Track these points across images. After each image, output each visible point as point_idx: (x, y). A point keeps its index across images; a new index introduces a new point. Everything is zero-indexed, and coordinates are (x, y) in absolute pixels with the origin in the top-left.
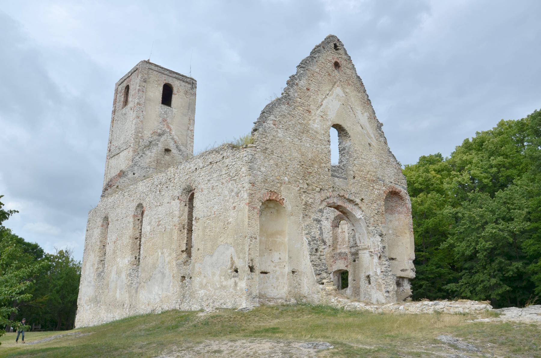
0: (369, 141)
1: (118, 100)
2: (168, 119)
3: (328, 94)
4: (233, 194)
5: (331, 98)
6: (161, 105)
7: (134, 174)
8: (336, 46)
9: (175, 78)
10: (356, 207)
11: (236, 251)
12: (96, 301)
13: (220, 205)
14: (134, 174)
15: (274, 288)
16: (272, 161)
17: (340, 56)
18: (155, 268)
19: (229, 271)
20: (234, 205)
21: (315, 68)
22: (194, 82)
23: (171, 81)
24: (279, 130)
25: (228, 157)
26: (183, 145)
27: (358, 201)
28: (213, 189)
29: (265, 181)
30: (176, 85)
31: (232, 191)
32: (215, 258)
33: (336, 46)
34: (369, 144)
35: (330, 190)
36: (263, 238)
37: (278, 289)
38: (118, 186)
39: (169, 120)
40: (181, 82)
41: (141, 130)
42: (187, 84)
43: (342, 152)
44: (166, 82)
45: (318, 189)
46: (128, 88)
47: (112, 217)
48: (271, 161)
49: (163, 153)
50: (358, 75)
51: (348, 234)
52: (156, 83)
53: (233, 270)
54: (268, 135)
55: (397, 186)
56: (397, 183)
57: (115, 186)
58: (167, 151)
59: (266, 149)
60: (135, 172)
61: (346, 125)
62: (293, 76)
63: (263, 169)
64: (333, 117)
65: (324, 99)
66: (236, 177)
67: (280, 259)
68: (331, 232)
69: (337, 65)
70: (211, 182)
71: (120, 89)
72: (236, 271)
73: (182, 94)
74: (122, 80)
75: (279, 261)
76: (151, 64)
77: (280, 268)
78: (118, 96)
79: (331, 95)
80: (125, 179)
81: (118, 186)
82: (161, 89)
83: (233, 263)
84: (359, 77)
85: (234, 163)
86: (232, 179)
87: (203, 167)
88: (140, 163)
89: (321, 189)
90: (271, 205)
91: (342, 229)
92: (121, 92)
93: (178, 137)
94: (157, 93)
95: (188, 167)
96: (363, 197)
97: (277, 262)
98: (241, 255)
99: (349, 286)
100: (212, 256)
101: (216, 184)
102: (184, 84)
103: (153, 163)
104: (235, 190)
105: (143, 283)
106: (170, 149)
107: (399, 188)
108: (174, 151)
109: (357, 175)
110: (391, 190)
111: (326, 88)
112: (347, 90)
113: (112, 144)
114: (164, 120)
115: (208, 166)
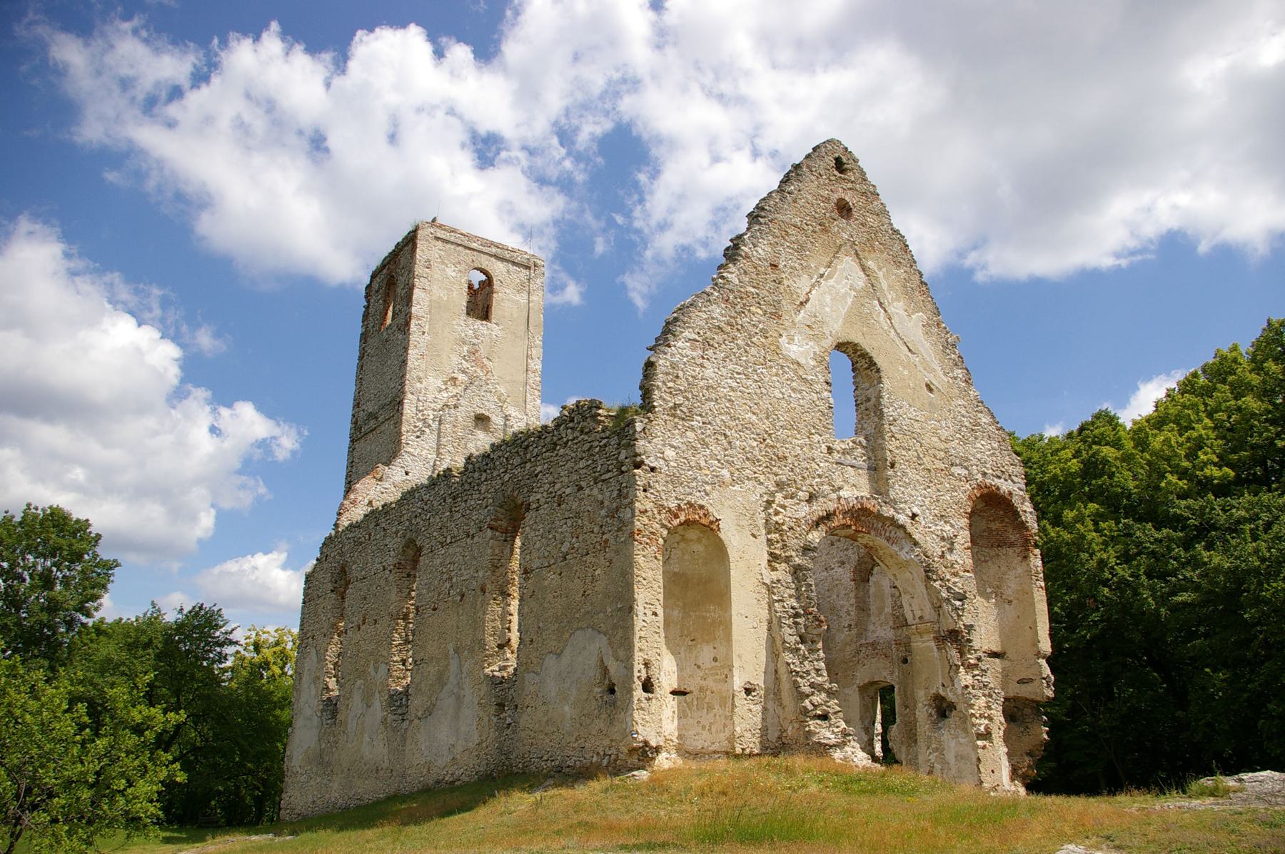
0: (930, 378)
3: (822, 276)
5: (831, 282)
6: (464, 317)
7: (407, 473)
8: (839, 165)
10: (900, 533)
11: (610, 643)
12: (322, 761)
14: (407, 473)
15: (704, 727)
17: (850, 185)
18: (443, 684)
19: (597, 690)
21: (789, 215)
23: (486, 262)
24: (706, 363)
27: (902, 519)
30: (498, 269)
32: (566, 659)
33: (839, 165)
34: (928, 386)
36: (676, 613)
37: (713, 730)
39: (483, 351)
41: (421, 375)
43: (863, 407)
46: (391, 283)
47: (355, 571)
48: (689, 433)
49: (471, 424)
50: (896, 226)
53: (605, 687)
54: (681, 374)
56: (999, 473)
57: (366, 501)
61: (867, 344)
62: (740, 237)
63: (670, 453)
64: (837, 328)
65: (813, 286)
67: (715, 660)
68: (852, 595)
69: (844, 209)
72: (612, 691)
75: (714, 664)
76: (441, 226)
77: (715, 681)
79: (830, 277)
83: (605, 671)
84: (896, 232)
85: (604, 441)
90: (692, 534)
96: (916, 510)
97: (708, 666)
98: (621, 653)
99: (898, 720)
100: (559, 655)
105: (416, 721)
106: (487, 414)
107: (1005, 486)
110: (985, 491)
111: (816, 261)
112: (870, 264)
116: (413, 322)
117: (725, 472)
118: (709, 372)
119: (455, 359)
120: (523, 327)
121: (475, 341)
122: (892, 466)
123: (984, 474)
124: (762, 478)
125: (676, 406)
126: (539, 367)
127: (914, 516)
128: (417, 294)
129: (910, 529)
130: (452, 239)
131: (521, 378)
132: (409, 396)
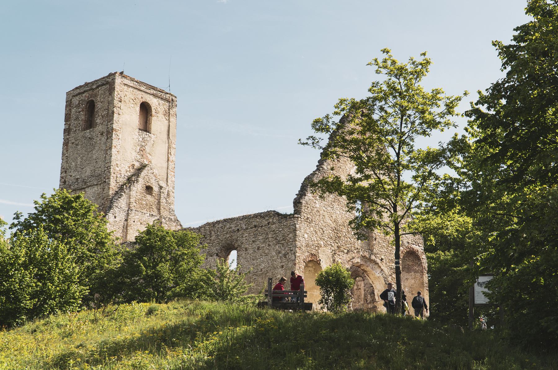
1: (73, 116)
4: (280, 255)
7: (115, 217)
9: (153, 95)
10: (376, 266)
13: (267, 264)
14: (115, 217)
16: (312, 229)
20: (282, 264)
22: (174, 98)
25: (274, 223)
27: (378, 261)
28: (258, 249)
29: (307, 246)
30: (154, 102)
31: (280, 252)
35: (355, 251)
44: (144, 100)
45: (346, 251)
51: (365, 290)
55: (414, 246)
56: (414, 243)
58: (149, 189)
59: (308, 218)
60: (116, 215)
63: (306, 236)
66: (283, 242)
70: (257, 243)
71: (76, 101)
73: (161, 115)
74: (78, 91)
78: (73, 110)
82: (138, 108)
86: (278, 242)
87: (247, 229)
89: (348, 251)
91: (358, 286)
92: (78, 106)
95: (228, 227)
96: (383, 257)
101: (263, 245)
104: (283, 252)
106: (151, 186)
107: (416, 247)
108: (156, 189)
109: (377, 237)
110: (408, 250)
113: (69, 174)
115: (251, 228)
116: (114, 132)
117: (322, 243)
118: (318, 206)
119: (134, 154)
120: (166, 136)
121: (143, 144)
122: (375, 239)
123: (409, 243)
124: (333, 245)
125: (308, 218)
127: (382, 259)
129: (380, 264)
130: (132, 85)
132: (112, 174)
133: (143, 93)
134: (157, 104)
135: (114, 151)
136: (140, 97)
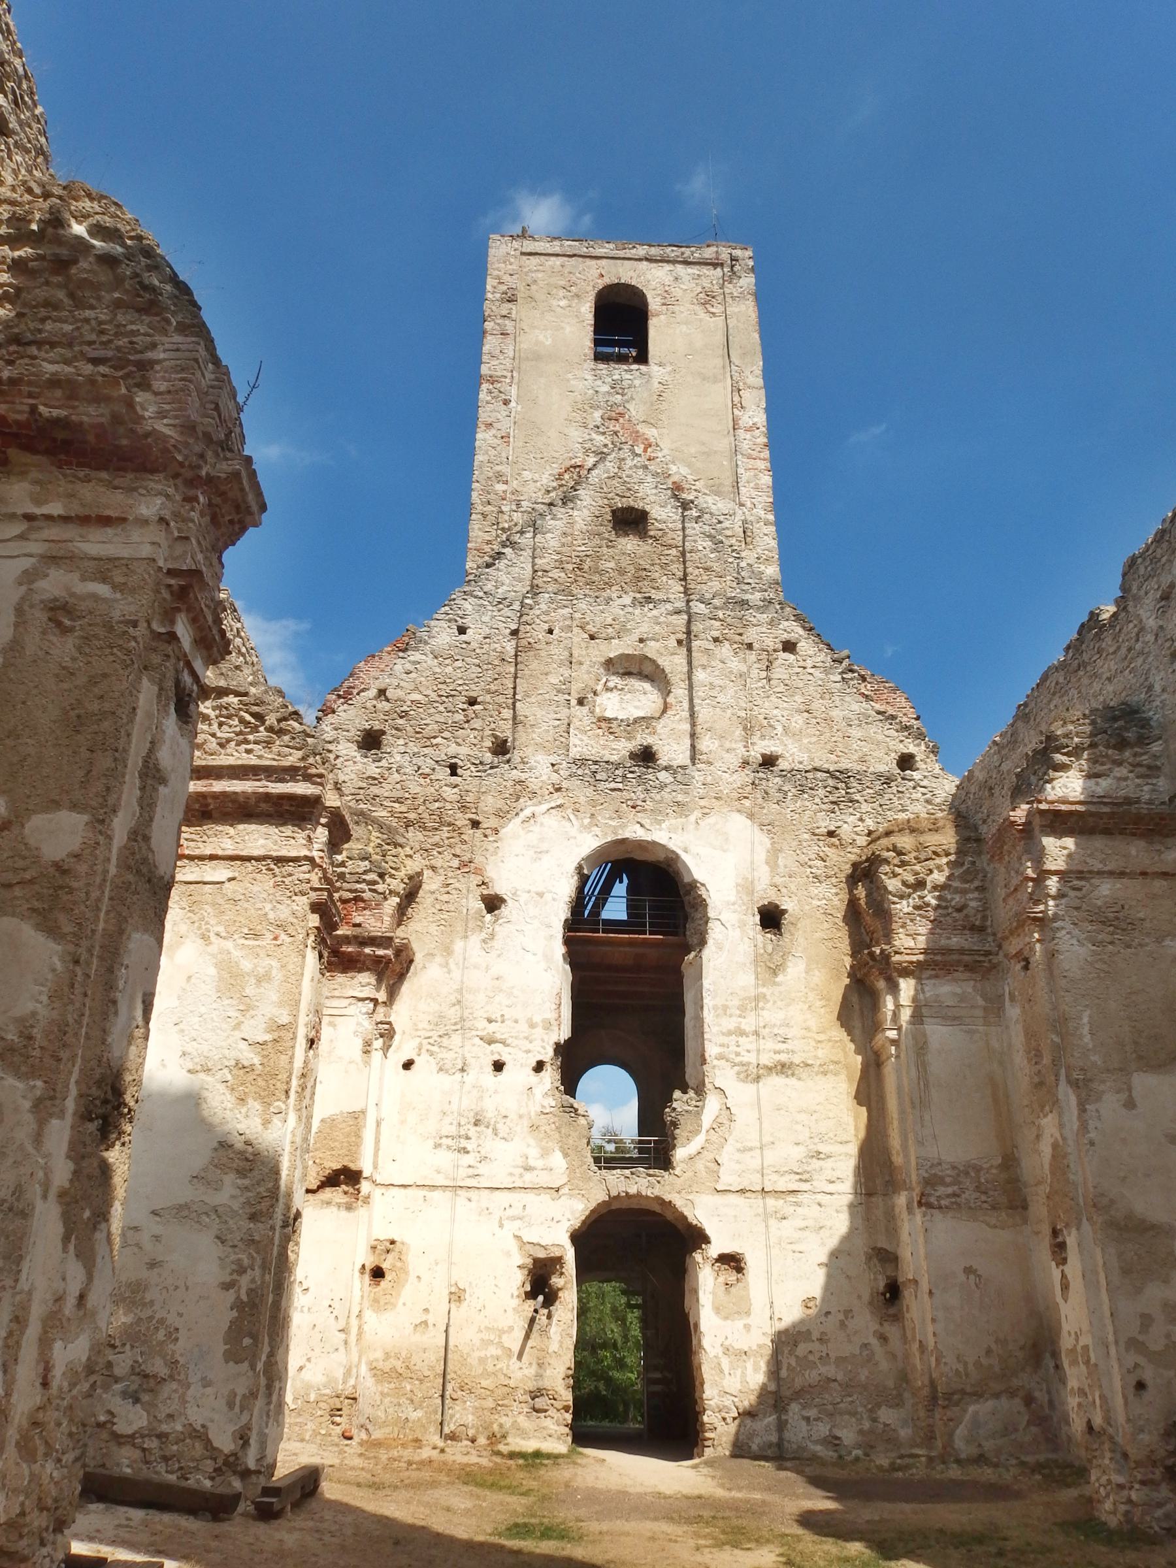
2: (630, 406)
6: (591, 364)
7: (462, 630)
14: (462, 630)
26: (718, 493)
38: (382, 692)
39: (635, 410)
40: (680, 268)
42: (707, 271)
49: (607, 531)
52: (562, 293)
57: (373, 692)
58: (630, 520)
60: (467, 622)
73: (685, 309)
80: (415, 656)
81: (382, 692)
88: (489, 587)
93: (689, 466)
94: (576, 325)
102: (694, 270)
103: (555, 574)
106: (639, 505)
108: (662, 513)
114: (615, 415)
116: (485, 386)
119: (576, 434)
126: (761, 418)
128: (490, 344)
130: (557, 250)
131: (725, 444)
133: (604, 262)
134: (668, 280)
135: (483, 437)
136: (596, 273)
